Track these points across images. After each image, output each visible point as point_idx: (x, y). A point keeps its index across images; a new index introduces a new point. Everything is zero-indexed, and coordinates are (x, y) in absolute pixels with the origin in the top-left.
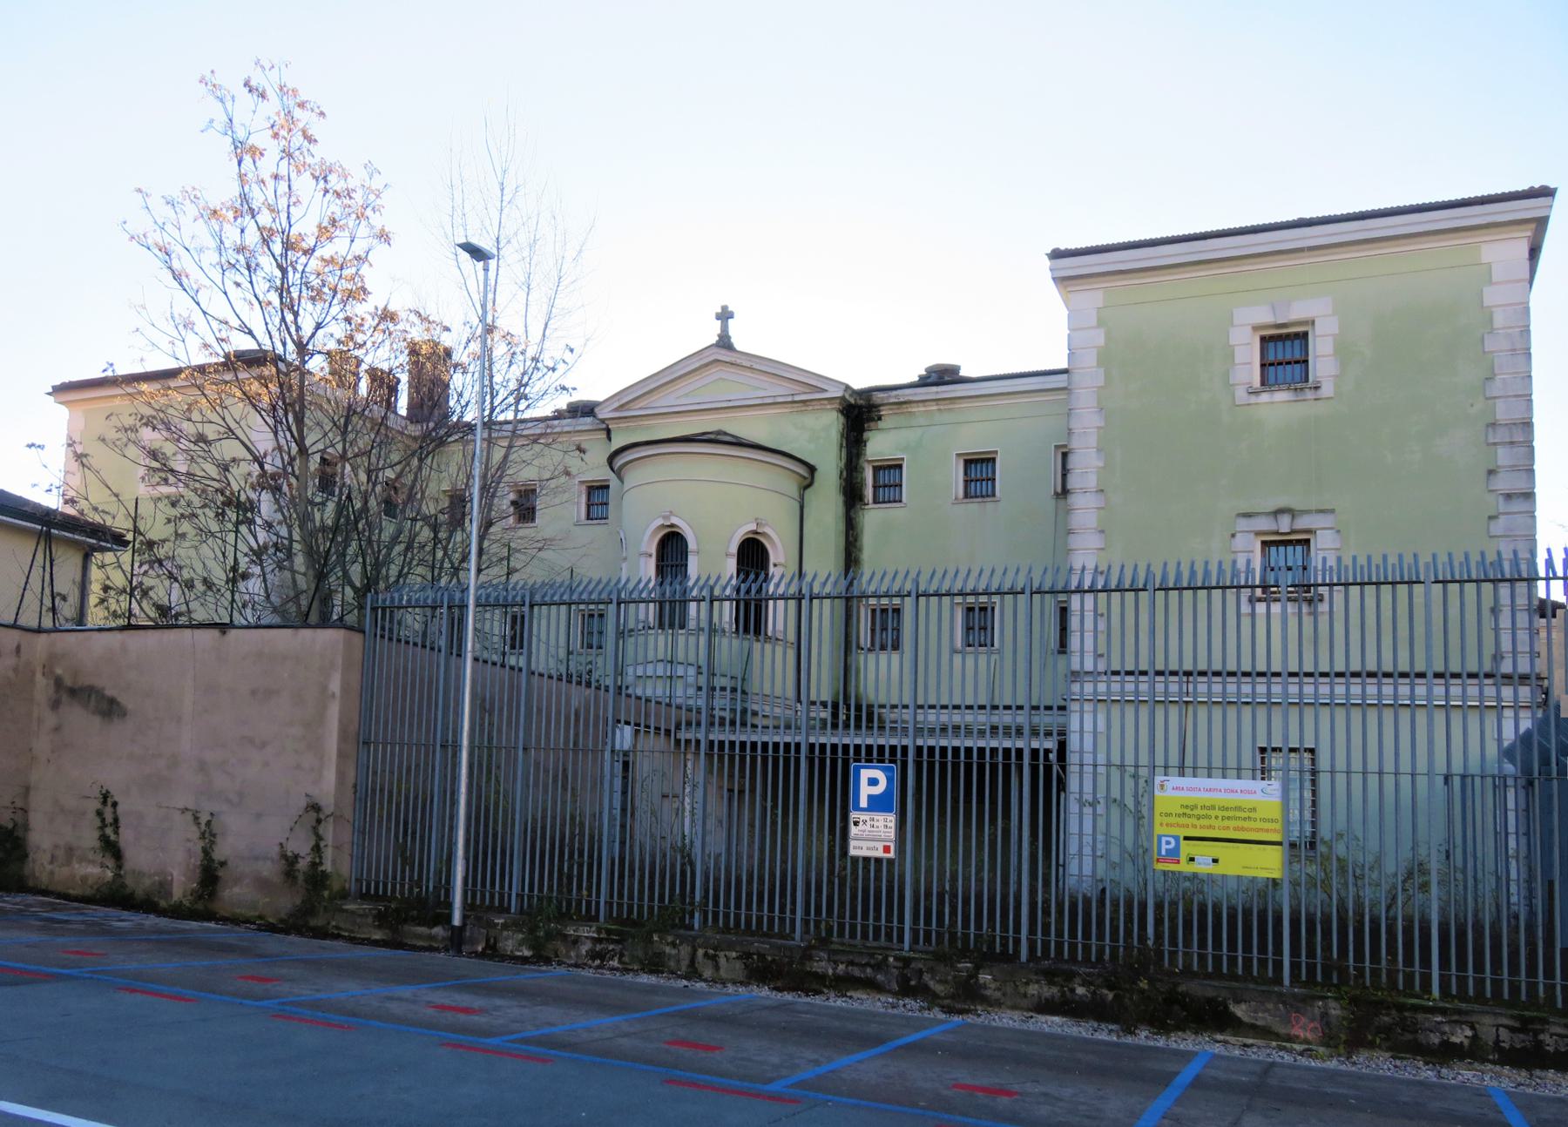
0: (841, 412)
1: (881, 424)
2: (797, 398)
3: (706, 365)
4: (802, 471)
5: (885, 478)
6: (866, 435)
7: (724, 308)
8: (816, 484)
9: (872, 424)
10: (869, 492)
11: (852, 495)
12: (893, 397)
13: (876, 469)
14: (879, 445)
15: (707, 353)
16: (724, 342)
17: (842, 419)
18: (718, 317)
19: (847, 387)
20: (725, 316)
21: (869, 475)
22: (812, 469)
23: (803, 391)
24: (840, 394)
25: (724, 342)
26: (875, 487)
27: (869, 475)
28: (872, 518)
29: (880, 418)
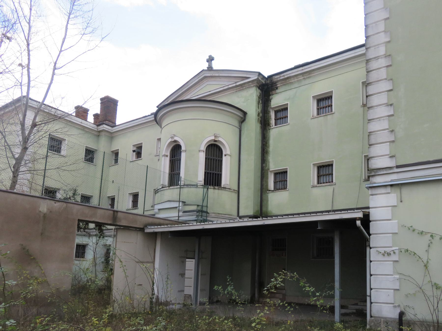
0: (259, 88)
1: (278, 91)
2: (238, 84)
3: (202, 80)
4: (240, 114)
5: (280, 115)
6: (271, 97)
7: (210, 56)
8: (247, 120)
9: (274, 92)
10: (273, 121)
11: (265, 124)
12: (282, 77)
13: (276, 112)
14: (277, 100)
15: (202, 74)
16: (210, 68)
17: (259, 91)
18: (208, 61)
19: (260, 74)
20: (210, 59)
21: (272, 115)
22: (245, 113)
23: (240, 80)
24: (256, 78)
25: (210, 68)
26: (275, 120)
27: (272, 115)
28: (275, 132)
29: (277, 88)
